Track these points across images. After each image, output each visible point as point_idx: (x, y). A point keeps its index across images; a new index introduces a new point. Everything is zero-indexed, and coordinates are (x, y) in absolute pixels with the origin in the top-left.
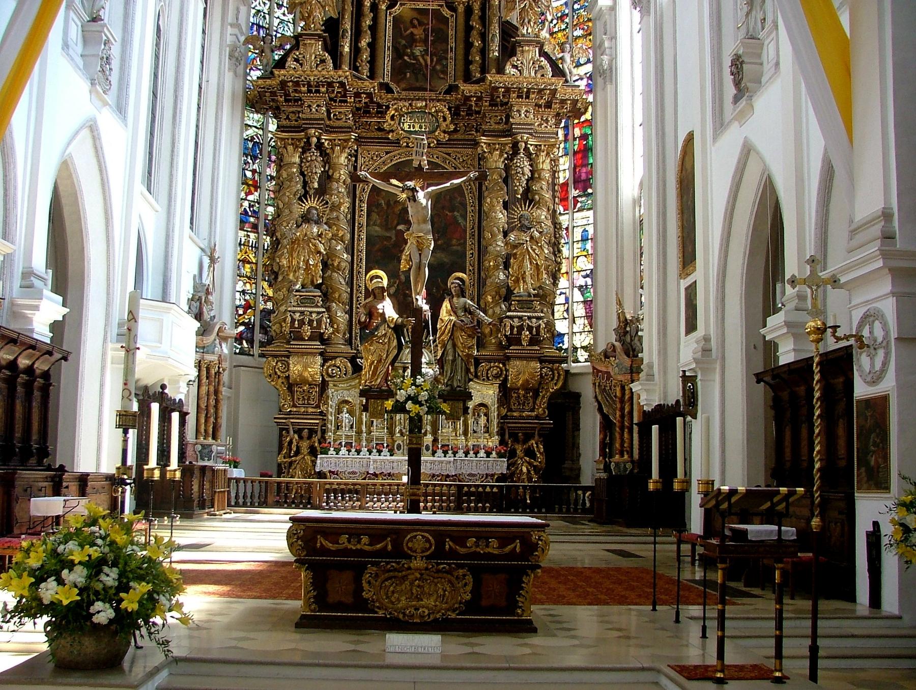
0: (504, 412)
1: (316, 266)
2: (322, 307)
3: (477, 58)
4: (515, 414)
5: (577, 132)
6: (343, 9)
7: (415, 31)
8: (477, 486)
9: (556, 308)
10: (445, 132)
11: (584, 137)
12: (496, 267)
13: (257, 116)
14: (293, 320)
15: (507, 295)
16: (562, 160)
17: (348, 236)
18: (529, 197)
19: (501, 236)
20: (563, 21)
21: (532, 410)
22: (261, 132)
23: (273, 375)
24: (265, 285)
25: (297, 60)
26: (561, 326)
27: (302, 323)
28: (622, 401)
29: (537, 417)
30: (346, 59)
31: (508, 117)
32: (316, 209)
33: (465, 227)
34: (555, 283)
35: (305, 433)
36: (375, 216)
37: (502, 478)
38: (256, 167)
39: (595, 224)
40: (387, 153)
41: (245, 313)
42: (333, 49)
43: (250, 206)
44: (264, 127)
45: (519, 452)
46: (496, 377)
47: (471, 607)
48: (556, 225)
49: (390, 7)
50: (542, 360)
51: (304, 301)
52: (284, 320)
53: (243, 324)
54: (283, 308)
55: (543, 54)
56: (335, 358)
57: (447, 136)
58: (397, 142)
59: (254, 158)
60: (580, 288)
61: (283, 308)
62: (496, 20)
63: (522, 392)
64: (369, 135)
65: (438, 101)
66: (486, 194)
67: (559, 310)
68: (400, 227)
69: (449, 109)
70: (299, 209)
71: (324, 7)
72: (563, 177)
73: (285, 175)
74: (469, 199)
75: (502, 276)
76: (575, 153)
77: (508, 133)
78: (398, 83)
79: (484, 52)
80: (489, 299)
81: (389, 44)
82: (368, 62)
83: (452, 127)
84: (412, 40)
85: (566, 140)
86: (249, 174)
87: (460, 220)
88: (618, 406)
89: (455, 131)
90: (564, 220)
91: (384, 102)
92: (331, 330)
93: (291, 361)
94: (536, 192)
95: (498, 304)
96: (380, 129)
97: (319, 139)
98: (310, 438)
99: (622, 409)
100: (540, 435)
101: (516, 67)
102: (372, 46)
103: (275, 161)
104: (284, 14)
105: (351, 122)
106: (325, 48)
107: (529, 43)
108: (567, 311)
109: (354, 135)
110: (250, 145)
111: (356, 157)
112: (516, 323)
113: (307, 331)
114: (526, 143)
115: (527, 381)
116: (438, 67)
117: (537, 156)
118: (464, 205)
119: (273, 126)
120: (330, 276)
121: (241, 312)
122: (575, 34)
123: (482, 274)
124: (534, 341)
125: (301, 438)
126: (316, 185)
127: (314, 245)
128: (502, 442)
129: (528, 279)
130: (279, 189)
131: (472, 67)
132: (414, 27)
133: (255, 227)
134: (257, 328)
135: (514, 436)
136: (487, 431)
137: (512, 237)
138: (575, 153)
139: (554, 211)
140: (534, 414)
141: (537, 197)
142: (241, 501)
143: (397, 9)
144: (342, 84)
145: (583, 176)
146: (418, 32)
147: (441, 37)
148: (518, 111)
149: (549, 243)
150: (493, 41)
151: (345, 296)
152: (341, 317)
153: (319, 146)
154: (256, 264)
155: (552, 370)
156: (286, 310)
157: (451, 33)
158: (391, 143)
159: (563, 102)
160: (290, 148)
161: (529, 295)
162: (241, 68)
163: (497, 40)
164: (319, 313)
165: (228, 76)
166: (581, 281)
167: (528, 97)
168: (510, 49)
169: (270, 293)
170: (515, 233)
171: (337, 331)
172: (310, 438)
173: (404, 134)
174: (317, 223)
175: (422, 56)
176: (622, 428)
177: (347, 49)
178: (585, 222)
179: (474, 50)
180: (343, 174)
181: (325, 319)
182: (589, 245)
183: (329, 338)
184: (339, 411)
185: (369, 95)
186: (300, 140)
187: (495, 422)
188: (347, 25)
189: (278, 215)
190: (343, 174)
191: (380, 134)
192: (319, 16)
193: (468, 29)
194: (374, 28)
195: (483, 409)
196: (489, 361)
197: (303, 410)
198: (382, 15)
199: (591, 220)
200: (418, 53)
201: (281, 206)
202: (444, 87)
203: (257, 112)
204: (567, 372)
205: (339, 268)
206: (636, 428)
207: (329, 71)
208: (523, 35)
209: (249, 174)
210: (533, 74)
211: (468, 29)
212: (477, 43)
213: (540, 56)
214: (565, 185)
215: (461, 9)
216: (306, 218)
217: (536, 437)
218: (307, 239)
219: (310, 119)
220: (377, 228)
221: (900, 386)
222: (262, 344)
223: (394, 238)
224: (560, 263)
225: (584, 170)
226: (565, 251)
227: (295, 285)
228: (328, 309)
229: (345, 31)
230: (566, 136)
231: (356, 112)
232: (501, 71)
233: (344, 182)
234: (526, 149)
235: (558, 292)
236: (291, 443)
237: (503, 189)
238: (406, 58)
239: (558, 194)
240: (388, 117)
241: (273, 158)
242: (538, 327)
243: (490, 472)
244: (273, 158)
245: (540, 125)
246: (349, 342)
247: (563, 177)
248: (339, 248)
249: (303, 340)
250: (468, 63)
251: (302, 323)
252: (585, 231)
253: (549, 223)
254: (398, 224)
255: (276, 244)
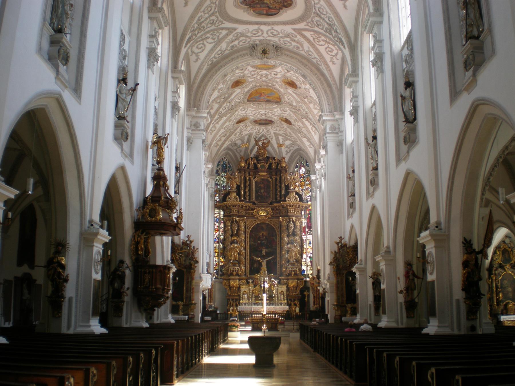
0: (288, 293)
1: (236, 255)
2: (239, 266)
3: (279, 194)
4: (291, 294)
5: (308, 212)
6: (241, 181)
7: (261, 185)
8: (281, 314)
9: (303, 263)
10: (270, 215)
11: (310, 214)
12: (285, 253)
13: (217, 210)
14: (231, 270)
15: (288, 261)
16: (303, 220)
17: (244, 246)
18: (294, 234)
19: (286, 245)
20: (303, 179)
21: (296, 293)
22: (218, 215)
23: (225, 285)
24: (221, 258)
25: (229, 198)
26: (304, 268)
27: (233, 271)
28: (317, 291)
29: (297, 295)
30: (243, 196)
31: (288, 212)
32: (236, 239)
33: (276, 241)
34: (302, 257)
35: (234, 300)
36: (251, 239)
37: (287, 311)
38: (218, 225)
39: (312, 239)
40: (254, 221)
41: (216, 267)
42: (239, 194)
43: (217, 236)
44: (219, 213)
45: (292, 304)
46: (286, 284)
47: (272, 328)
48: (302, 240)
49: (254, 178)
50: (298, 279)
51: (234, 265)
52: (228, 270)
53: (216, 270)
54: (227, 266)
55: (297, 194)
56: (242, 280)
57: (271, 216)
58: (257, 218)
59: (217, 222)
60: (309, 257)
61: (227, 266)
62: (283, 183)
63: (292, 288)
64: (249, 216)
65: (269, 207)
66: (282, 233)
67: (303, 263)
68: (259, 242)
69: (271, 209)
70: (230, 239)
71: (236, 182)
72: (303, 225)
73: (226, 229)
74: (277, 233)
75: (287, 256)
76: (307, 218)
77: (287, 216)
78: (257, 201)
79: (281, 192)
80: (283, 262)
81: (254, 189)
82: (248, 195)
83: (272, 214)
84: (260, 188)
85: (305, 214)
86: (216, 227)
87: (275, 239)
88: (316, 292)
89: (273, 214)
90: (304, 237)
91: (253, 207)
92: (241, 272)
93: (231, 281)
94: (296, 232)
95: (286, 263)
96: (252, 214)
97: (236, 219)
98: (236, 302)
99: (317, 293)
100: (298, 299)
101: (289, 198)
102: (249, 191)
103: (223, 223)
104: (224, 179)
105: (244, 214)
106: (237, 195)
107: (292, 192)
108: (306, 263)
109: (245, 218)
110: (216, 219)
111: (246, 222)
112: (290, 269)
113: (235, 273)
114: (292, 219)
115: (294, 285)
116: (268, 196)
117: (296, 222)
118: (276, 235)
119: (222, 213)
120: (240, 257)
121: (215, 267)
122: (307, 183)
123: (282, 255)
124: (296, 274)
125: (233, 302)
126: (235, 232)
127: (236, 250)
128: (287, 302)
129: (294, 258)
130: (225, 232)
131: (278, 196)
132: (261, 184)
133: (218, 242)
134: (219, 271)
135: (291, 300)
136: (284, 299)
137: (289, 246)
138: (307, 218)
139: (301, 236)
140: (296, 294)
141: (296, 233)
142: (223, 319)
143: (256, 179)
144: (242, 205)
145: (310, 225)
146: (262, 186)
147: (269, 187)
148: (290, 210)
149: (300, 246)
150: (283, 189)
151: (244, 262)
152: (243, 268)
153: (236, 221)
154: (218, 252)
155: (301, 282)
156: (228, 267)
157: (271, 185)
158: (254, 218)
159: (303, 207)
160: (228, 222)
161: (294, 262)
162: (213, 198)
163: (284, 189)
164: (238, 268)
165: (211, 202)
166: (309, 255)
167: (292, 206)
168: (287, 193)
169: (222, 260)
170: (290, 244)
171: (242, 272)
172: (236, 302)
173: (259, 216)
174: (237, 243)
175: (263, 193)
176: (317, 298)
177: (242, 193)
178: (310, 238)
179: (278, 191)
180: (242, 228)
181: (239, 270)
182: (311, 245)
183: (240, 274)
184: (243, 294)
185: (249, 207)
186: (230, 219)
187: (286, 296)
188: (243, 186)
189: (224, 239)
190: (242, 228)
191: (252, 216)
192: (235, 186)
193: (276, 185)
194: (250, 185)
195: (283, 293)
196: (284, 279)
197: (234, 294)
198: (252, 181)
199: (312, 238)
200: (262, 192)
201: (226, 237)
202: (269, 202)
203: (217, 209)
204: (306, 281)
205: (242, 255)
206: (320, 298)
207: (238, 202)
208: (291, 190)
209: (216, 227)
210: (293, 200)
211: (276, 185)
212: (279, 189)
213: (296, 195)
214: (304, 228)
215: (274, 179)
216: (233, 242)
217: (297, 300)
218: (234, 248)
219: (234, 214)
220: (252, 242)
221: (330, 299)
222: (221, 275)
223: (257, 245)
224: (303, 251)
225: (310, 223)
226: (305, 247)
227: (231, 260)
228: (239, 266)
229: (242, 188)
230: (305, 213)
231: (245, 210)
232: (285, 201)
233: (243, 231)
234: (293, 220)
235: (303, 258)
236: (230, 303)
237: (286, 232)
238: (259, 193)
239: (302, 231)
240: (254, 212)
241: (222, 222)
242: (296, 271)
243: (284, 310)
244: (222, 222)
245: (296, 213)
246: (245, 275)
247: (303, 225)
248: (242, 249)
249: (233, 275)
250: (276, 195)
251: (233, 271)
252: (310, 241)
253: (299, 241)
254: (258, 241)
255: (224, 248)
